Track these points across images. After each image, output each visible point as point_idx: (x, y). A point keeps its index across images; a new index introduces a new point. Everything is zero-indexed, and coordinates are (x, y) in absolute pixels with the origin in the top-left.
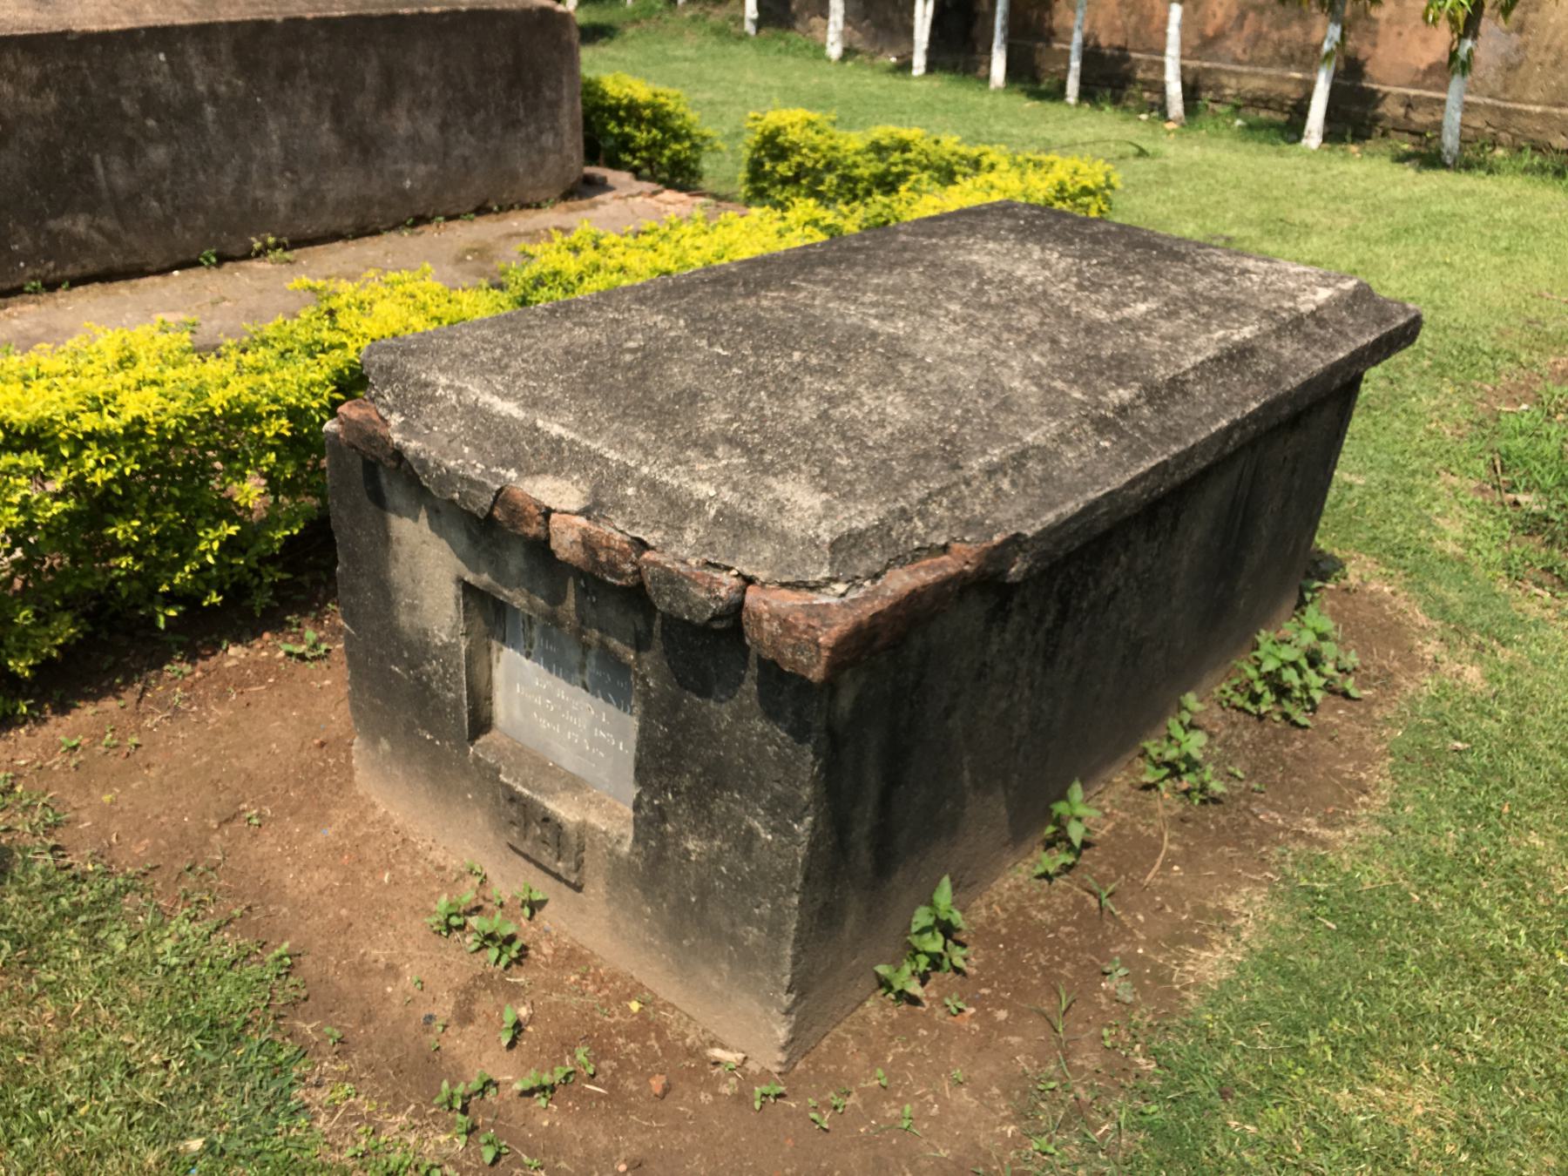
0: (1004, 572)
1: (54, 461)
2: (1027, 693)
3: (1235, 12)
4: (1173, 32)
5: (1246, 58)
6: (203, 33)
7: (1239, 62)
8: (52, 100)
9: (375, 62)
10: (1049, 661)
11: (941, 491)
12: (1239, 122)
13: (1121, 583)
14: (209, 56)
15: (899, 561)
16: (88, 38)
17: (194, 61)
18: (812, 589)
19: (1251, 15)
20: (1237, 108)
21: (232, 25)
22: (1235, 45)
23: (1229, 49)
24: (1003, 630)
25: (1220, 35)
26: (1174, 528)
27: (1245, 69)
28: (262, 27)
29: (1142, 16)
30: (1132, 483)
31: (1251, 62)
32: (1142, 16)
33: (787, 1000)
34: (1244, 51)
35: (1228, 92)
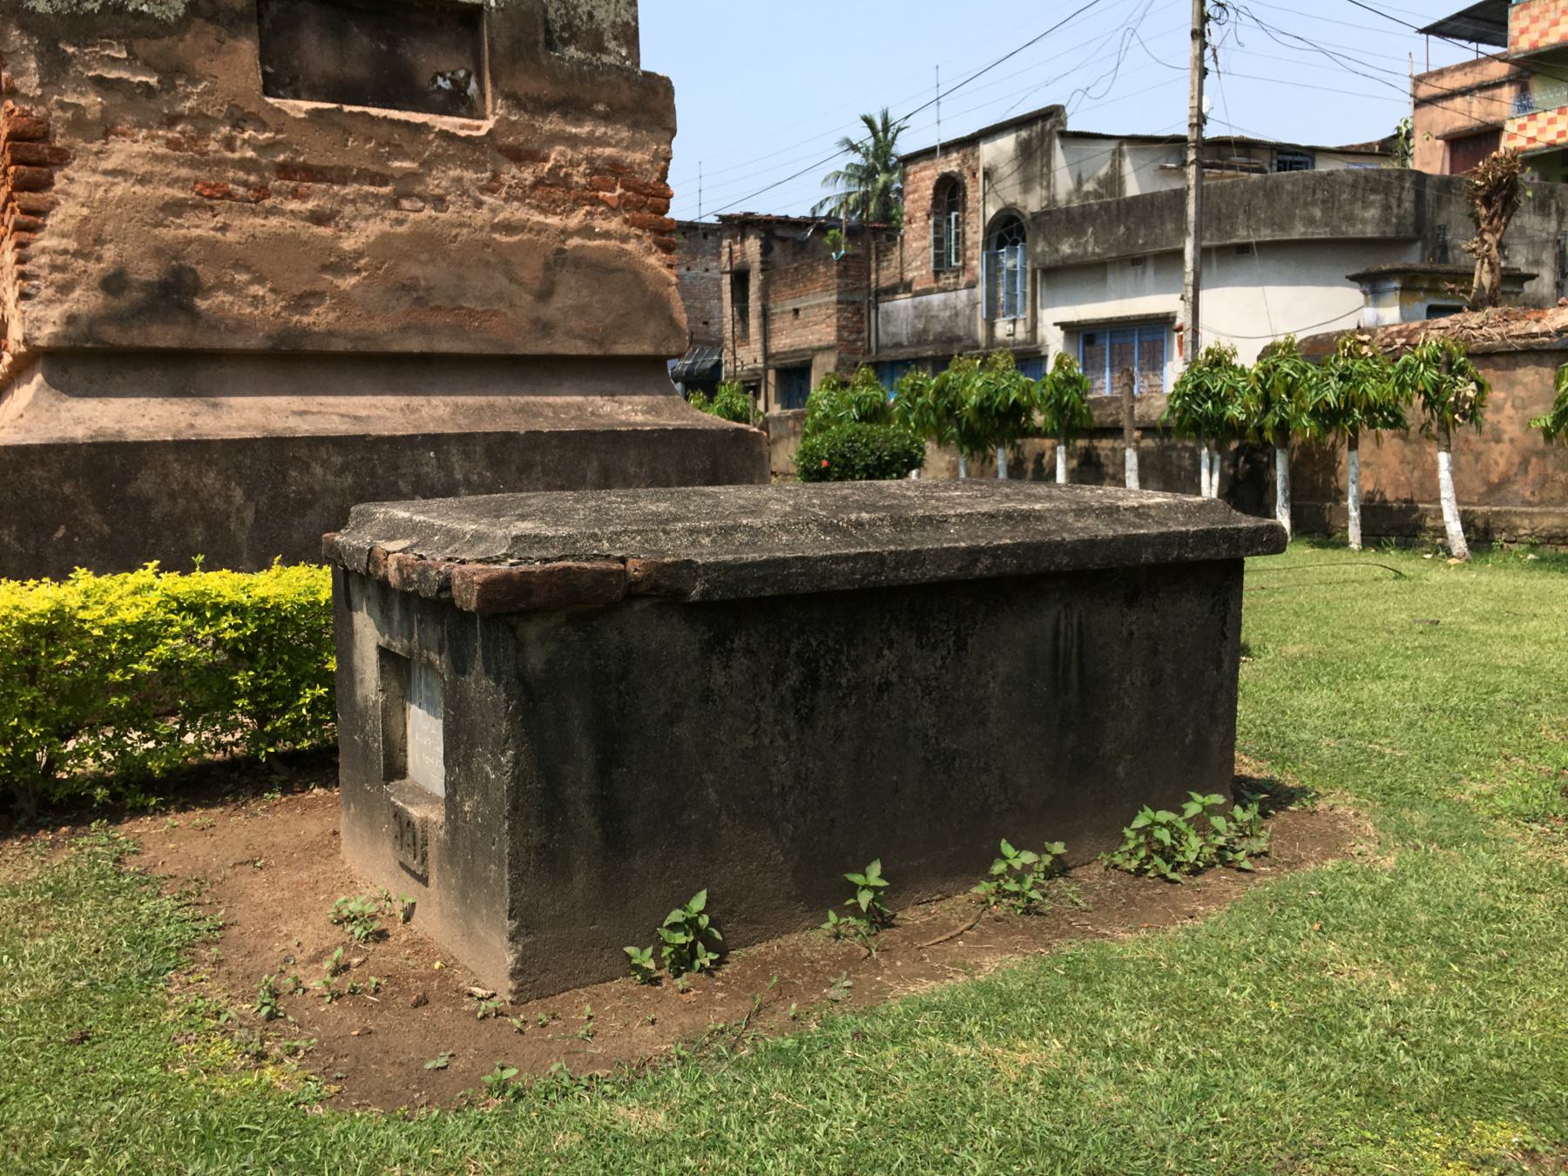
0: (685, 594)
1: (202, 622)
2: (780, 742)
3: (1517, 459)
4: (1445, 476)
5: (1536, 499)
6: (464, 439)
7: (1530, 504)
8: (349, 479)
9: (595, 464)
10: (806, 720)
11: (638, 532)
12: (1531, 556)
13: (894, 677)
14: (467, 455)
15: (573, 557)
16: (380, 440)
17: (455, 456)
18: (495, 562)
19: (1534, 460)
20: (1533, 545)
21: (487, 434)
22: (1523, 488)
23: (1516, 493)
24: (727, 667)
25: (1505, 481)
26: (961, 646)
27: (1536, 510)
28: (509, 436)
29: (1424, 470)
30: (836, 559)
31: (1541, 503)
32: (1424, 470)
33: (510, 925)
34: (1533, 493)
35: (1522, 532)
